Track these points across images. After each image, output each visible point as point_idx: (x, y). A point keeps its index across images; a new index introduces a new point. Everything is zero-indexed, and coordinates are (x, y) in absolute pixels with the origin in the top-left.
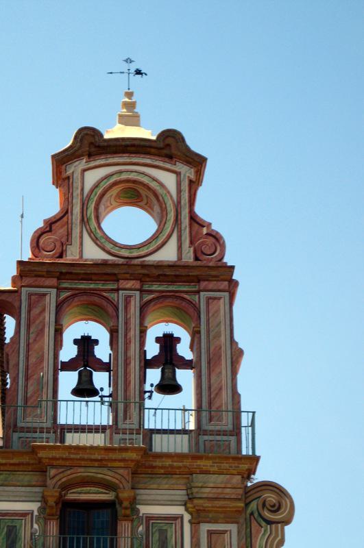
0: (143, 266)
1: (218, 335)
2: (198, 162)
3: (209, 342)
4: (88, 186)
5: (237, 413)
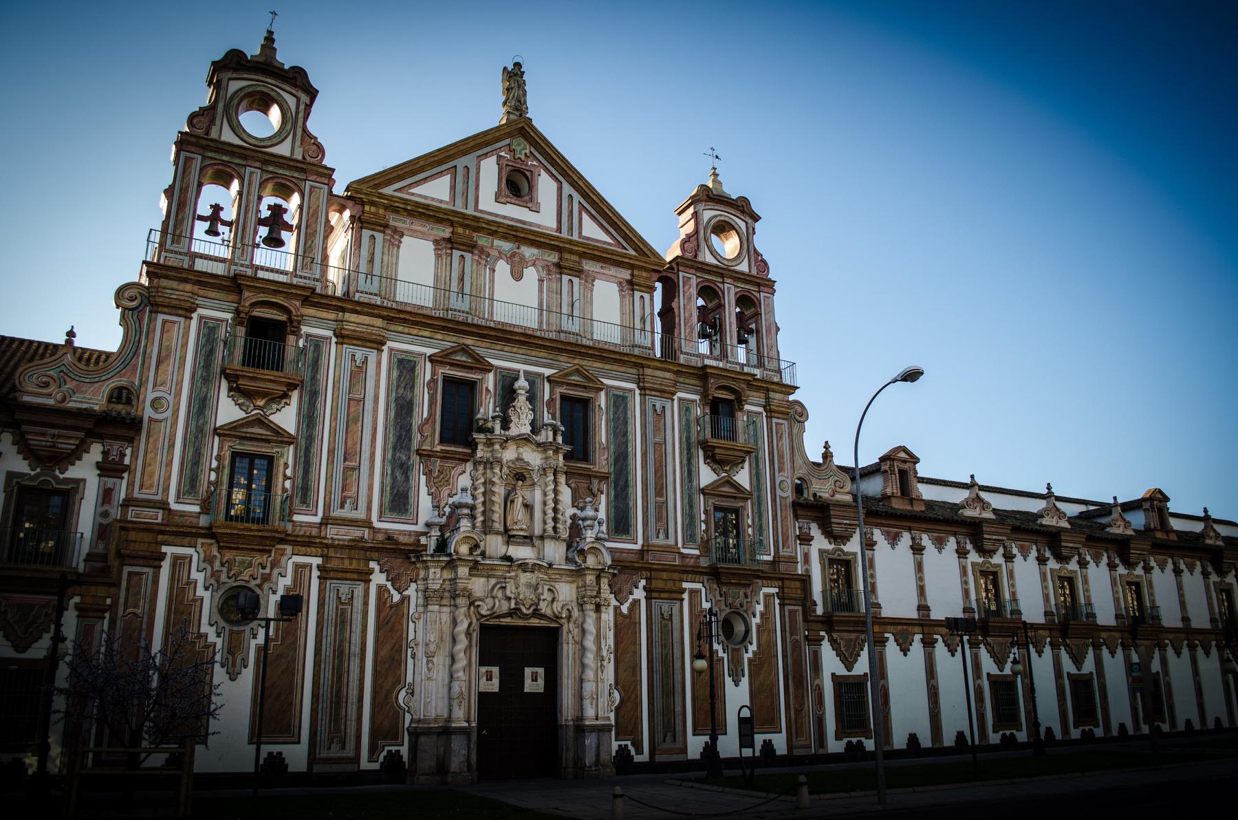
0: (737, 272)
2: (756, 218)
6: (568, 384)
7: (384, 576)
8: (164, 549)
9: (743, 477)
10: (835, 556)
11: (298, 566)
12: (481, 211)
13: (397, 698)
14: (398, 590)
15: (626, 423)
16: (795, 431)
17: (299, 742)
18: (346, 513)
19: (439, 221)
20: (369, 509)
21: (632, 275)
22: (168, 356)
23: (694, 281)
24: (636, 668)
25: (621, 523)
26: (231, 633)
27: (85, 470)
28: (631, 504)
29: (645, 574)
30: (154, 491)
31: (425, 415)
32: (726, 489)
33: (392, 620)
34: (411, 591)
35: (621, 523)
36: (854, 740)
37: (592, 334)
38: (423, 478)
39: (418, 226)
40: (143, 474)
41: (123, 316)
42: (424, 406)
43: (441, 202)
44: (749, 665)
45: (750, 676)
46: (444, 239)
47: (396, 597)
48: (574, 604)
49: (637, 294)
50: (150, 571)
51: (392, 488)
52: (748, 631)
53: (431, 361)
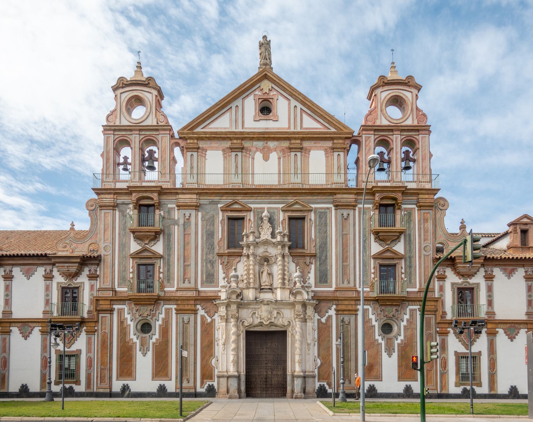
1: (425, 150)
2: (418, 88)
3: (422, 152)
4: (383, 98)
5: (431, 175)
6: (292, 211)
7: (203, 311)
8: (114, 306)
9: (400, 248)
10: (462, 286)
11: (166, 309)
12: (246, 128)
14: (209, 316)
15: (326, 225)
16: (438, 216)
17: (171, 380)
18: (186, 285)
19: (224, 139)
21: (333, 143)
22: (108, 228)
23: (372, 138)
24: (329, 348)
25: (323, 278)
26: (142, 338)
27: (83, 279)
28: (329, 268)
30: (108, 284)
31: (220, 237)
32: (388, 254)
33: (208, 330)
34: (216, 317)
35: (323, 278)
36: (468, 388)
37: (309, 181)
38: (220, 266)
39: (214, 144)
40: (104, 278)
41: (90, 214)
42: (220, 232)
43: (225, 128)
44: (398, 346)
45: (398, 351)
47: (209, 320)
49: (336, 154)
50: (109, 315)
51: (206, 272)
52: (399, 329)
53: (222, 210)
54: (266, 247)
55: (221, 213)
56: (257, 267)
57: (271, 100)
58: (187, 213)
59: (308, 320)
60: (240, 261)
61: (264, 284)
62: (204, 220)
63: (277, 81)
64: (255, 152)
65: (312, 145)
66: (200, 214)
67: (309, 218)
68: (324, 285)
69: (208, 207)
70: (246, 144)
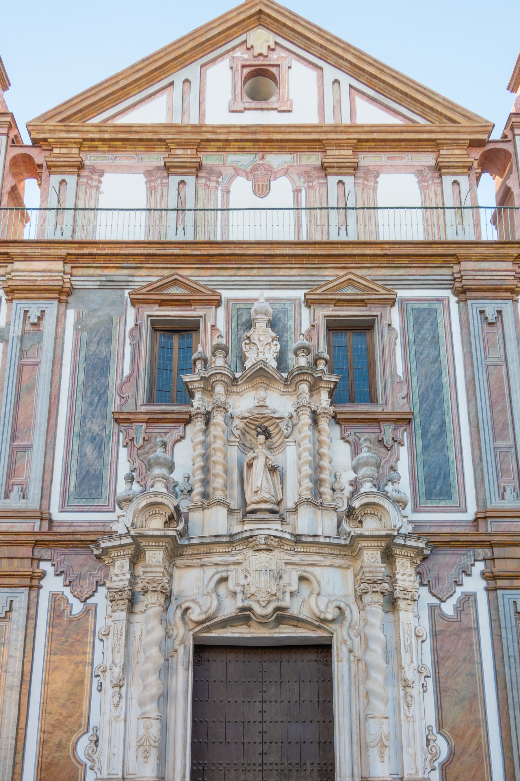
13: (74, 749)
15: (436, 342)
20: (45, 494)
24: (476, 698)
25: (437, 484)
28: (452, 456)
29: (481, 552)
31: (127, 371)
34: (100, 598)
35: (437, 484)
38: (123, 452)
39: (123, 159)
46: (158, 168)
48: (351, 600)
51: (80, 467)
54: (262, 393)
55: (131, 311)
56: (234, 452)
57: (274, 70)
58: (34, 309)
59: (402, 604)
60: (182, 438)
61: (257, 498)
62: (82, 330)
63: (289, 23)
64: (233, 178)
65: (383, 163)
66: (71, 315)
67: (385, 323)
68: (443, 503)
69: (97, 296)
70: (210, 159)
